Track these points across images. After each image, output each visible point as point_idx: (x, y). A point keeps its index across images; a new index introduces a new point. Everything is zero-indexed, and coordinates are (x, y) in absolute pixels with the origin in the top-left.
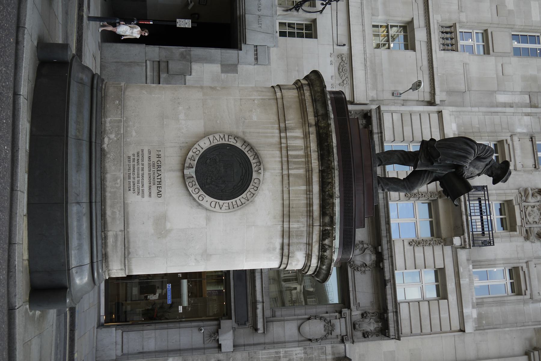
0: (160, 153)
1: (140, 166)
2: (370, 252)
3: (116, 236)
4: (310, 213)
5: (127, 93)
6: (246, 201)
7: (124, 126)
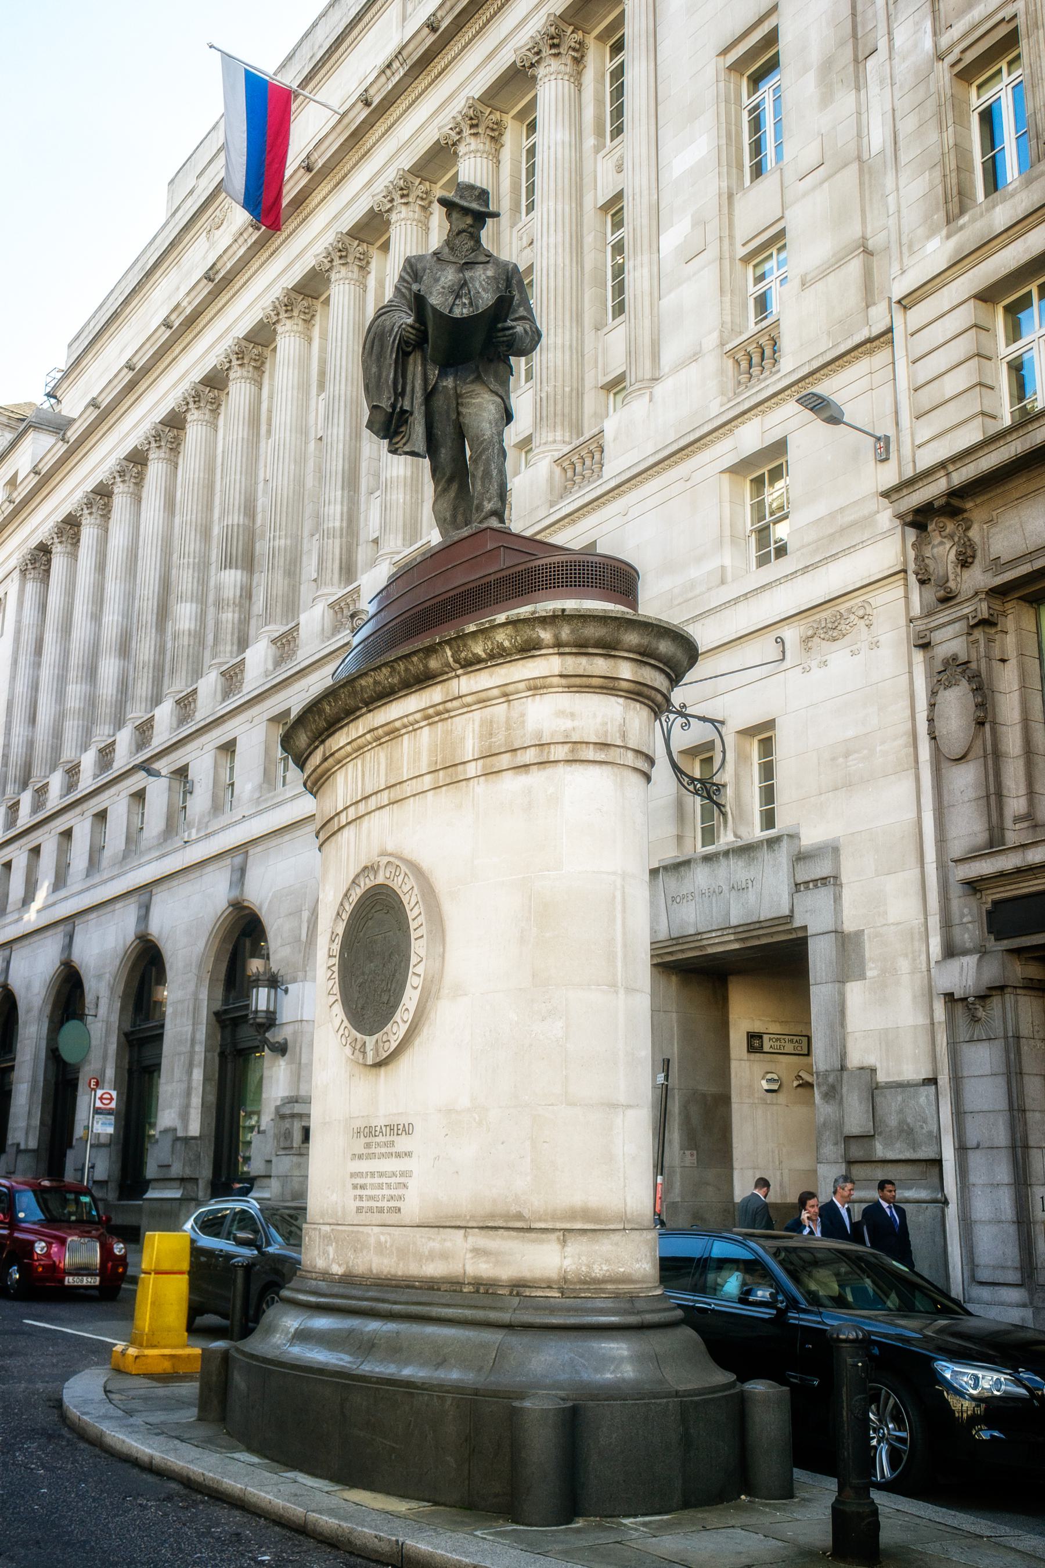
3: (477, 1252)
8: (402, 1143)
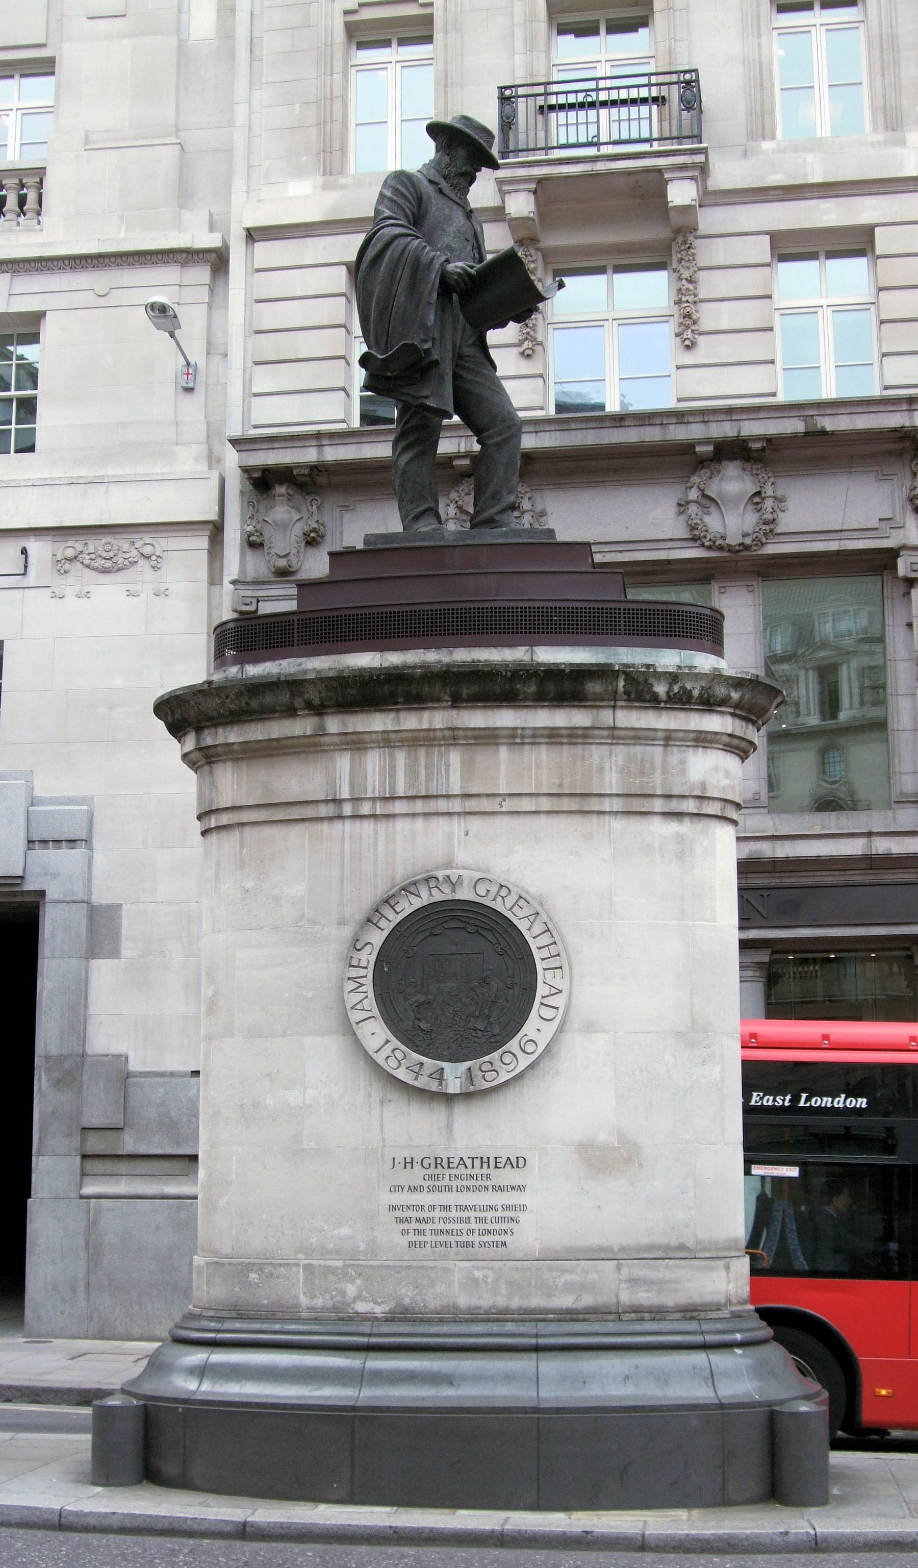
0: (399, 1159)
1: (437, 1214)
2: (716, 480)
4: (577, 736)
5: (227, 1249)
6: (538, 919)
7: (324, 1258)
8: (507, 1176)
